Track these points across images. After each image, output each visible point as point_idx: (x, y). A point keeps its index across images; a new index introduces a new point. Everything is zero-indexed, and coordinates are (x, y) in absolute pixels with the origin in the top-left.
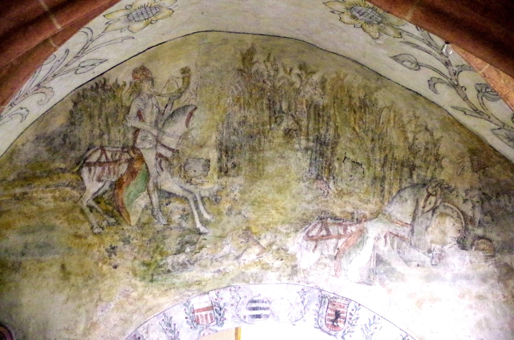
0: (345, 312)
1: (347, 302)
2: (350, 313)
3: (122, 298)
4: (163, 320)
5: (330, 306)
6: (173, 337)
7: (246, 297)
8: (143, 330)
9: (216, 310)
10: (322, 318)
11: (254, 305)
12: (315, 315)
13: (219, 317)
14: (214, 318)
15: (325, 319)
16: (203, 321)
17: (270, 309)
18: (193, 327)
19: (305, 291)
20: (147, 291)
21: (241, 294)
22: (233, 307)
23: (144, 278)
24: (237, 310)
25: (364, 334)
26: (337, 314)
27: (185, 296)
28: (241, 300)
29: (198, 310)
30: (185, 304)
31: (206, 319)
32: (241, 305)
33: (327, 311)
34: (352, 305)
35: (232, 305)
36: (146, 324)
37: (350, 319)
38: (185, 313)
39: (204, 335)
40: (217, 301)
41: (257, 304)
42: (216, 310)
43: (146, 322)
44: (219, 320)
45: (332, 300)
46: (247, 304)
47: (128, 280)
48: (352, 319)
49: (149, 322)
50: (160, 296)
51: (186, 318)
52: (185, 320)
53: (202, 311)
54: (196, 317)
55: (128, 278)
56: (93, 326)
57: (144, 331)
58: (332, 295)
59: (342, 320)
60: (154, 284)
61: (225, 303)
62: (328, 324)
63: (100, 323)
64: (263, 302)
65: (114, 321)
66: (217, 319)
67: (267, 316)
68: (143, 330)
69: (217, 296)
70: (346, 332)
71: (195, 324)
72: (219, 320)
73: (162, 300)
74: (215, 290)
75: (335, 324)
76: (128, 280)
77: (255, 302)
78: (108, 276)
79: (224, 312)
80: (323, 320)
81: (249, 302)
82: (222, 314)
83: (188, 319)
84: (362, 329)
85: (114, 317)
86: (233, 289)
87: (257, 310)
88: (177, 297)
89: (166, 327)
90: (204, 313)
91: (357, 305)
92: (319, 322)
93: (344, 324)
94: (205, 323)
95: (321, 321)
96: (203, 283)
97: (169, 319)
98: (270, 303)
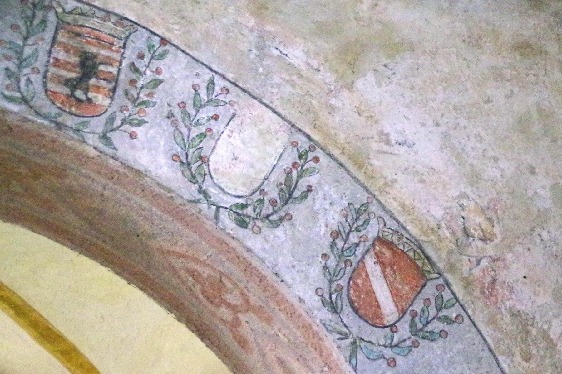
2: (133, 64)
5: (62, 38)
10: (36, 71)
12: (8, 58)
15: (45, 77)
25: (177, 133)
33: (50, 52)
37: (133, 82)
45: (69, 19)
48: (139, 85)
59: (103, 83)
62: (54, 93)
70: (118, 122)
75: (79, 93)
80: (36, 79)
84: (170, 116)
91: (156, 41)
92: (23, 84)
93: (112, 98)
95: (28, 80)
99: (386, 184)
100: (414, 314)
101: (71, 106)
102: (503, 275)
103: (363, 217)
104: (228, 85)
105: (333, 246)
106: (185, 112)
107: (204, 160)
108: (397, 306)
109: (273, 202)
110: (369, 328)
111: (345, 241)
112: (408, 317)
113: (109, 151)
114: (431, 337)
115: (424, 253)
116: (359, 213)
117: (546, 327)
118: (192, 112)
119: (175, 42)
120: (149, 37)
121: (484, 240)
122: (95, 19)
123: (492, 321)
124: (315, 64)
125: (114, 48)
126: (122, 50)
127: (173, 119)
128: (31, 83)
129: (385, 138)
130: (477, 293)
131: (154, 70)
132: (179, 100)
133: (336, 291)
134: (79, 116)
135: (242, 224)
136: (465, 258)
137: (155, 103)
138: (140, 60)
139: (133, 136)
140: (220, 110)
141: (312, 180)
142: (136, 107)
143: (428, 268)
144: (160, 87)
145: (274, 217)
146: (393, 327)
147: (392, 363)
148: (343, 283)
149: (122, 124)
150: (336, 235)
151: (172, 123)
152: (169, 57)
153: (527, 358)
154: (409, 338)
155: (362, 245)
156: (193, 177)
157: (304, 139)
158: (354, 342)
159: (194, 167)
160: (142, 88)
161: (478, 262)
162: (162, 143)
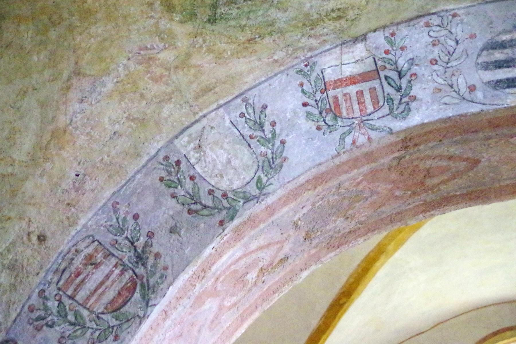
3: (132, 66)
4: (242, 115)
6: (270, 156)
7: (473, 36)
8: (189, 143)
9: (386, 77)
11: (499, 55)
14: (381, 98)
20: (201, 47)
22: (436, 67)
23: (193, 16)
24: (450, 71)
27: (303, 48)
28: (460, 48)
29: (339, 83)
30: (300, 71)
32: (459, 58)
35: (433, 62)
36: (198, 127)
38: (301, 94)
39: (354, 142)
40: (390, 56)
41: (508, 51)
42: (386, 77)
43: (197, 121)
44: (396, 102)
46: (479, 55)
47: (152, 21)
49: (204, 122)
50: (237, 54)
51: (305, 105)
52: (302, 111)
53: (347, 85)
54: (331, 100)
55: (151, 17)
57: (192, 145)
60: (219, 27)
61: (412, 59)
63: (76, 129)
65: (113, 123)
66: (390, 100)
68: (189, 143)
69: (391, 43)
71: (329, 119)
72: (396, 102)
74: (384, 27)
76: (152, 21)
78: (99, 15)
79: (410, 82)
81: (482, 50)
82: (404, 86)
83: (308, 108)
89: (251, 133)
90: (353, 89)
94: (357, 114)
96: (351, 14)
97: (258, 111)
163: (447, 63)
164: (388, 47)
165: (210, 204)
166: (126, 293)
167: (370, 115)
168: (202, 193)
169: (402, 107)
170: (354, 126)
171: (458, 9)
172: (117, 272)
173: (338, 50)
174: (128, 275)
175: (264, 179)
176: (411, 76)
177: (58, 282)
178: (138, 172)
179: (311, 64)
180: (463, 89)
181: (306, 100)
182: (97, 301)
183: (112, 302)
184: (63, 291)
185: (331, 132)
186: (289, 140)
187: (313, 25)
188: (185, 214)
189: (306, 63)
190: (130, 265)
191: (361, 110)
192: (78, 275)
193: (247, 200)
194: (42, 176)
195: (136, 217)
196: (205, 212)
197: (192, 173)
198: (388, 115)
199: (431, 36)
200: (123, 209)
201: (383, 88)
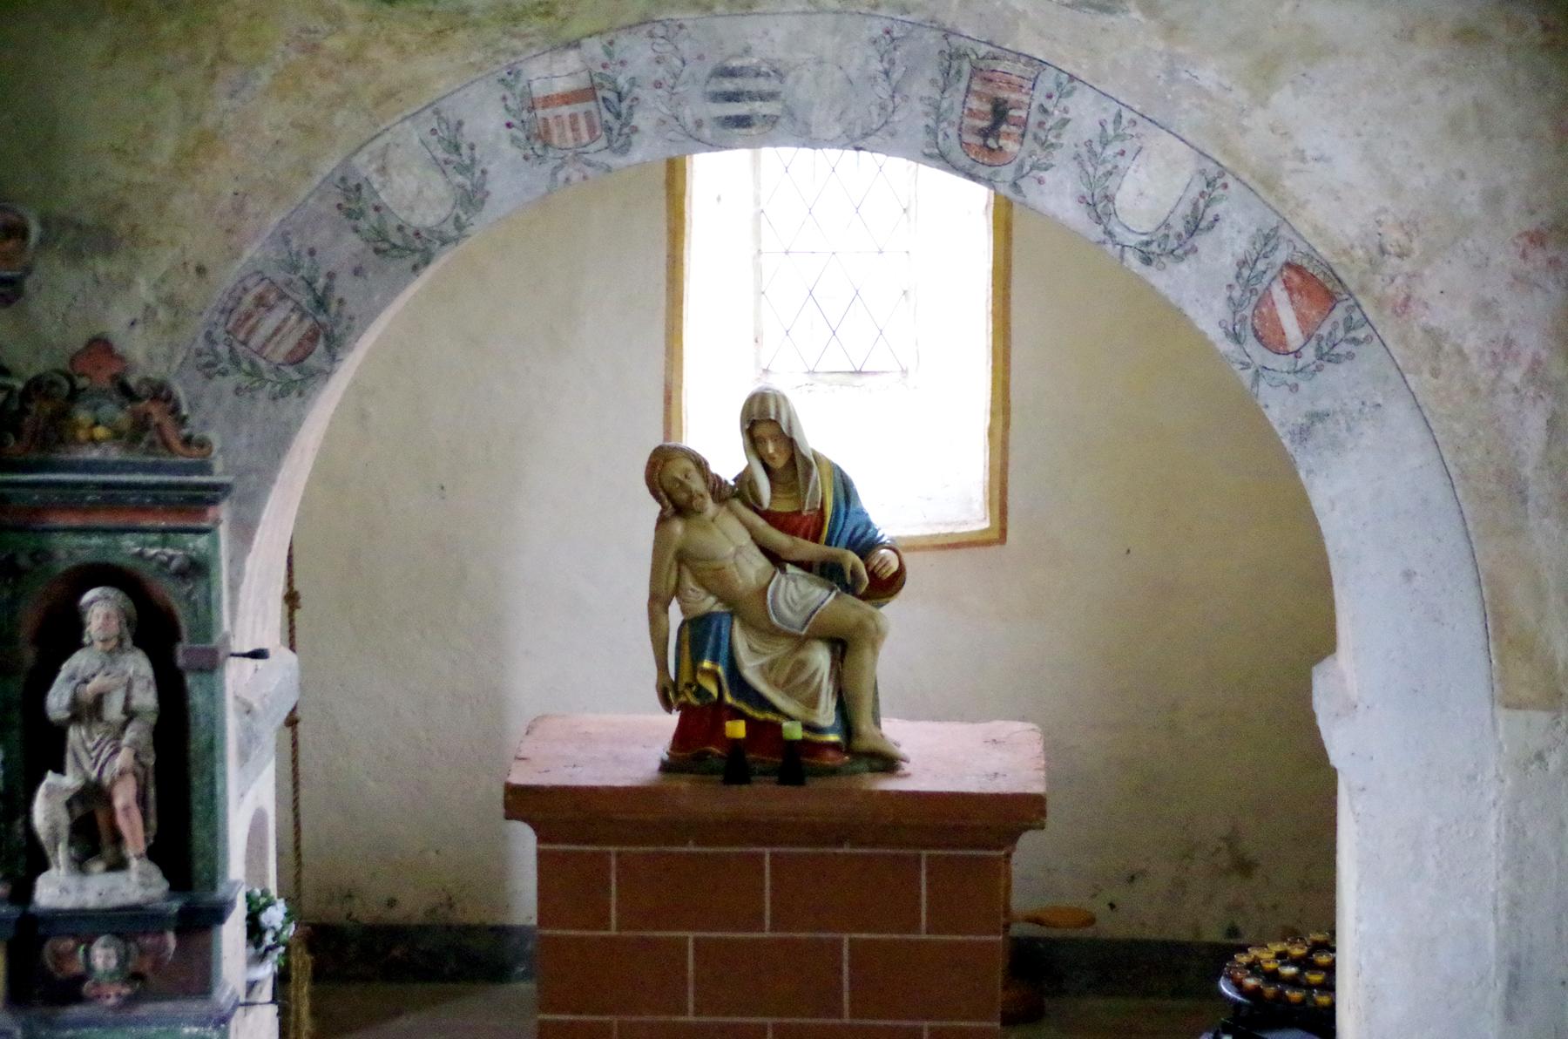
0: (1025, 105)
1: (1030, 72)
2: (1042, 105)
3: (293, 56)
4: (434, 131)
7: (700, 57)
8: (370, 161)
9: (604, 99)
10: (951, 124)
11: (729, 85)
12: (927, 114)
13: (616, 125)
15: (960, 129)
16: (562, 135)
17: (782, 96)
18: (533, 158)
19: (895, 34)
21: (685, 46)
22: (659, 92)
26: (1000, 112)
27: (503, 51)
28: (687, 70)
29: (548, 101)
30: (502, 80)
31: (574, 129)
32: (685, 83)
33: (964, 102)
34: (1047, 82)
35: (658, 85)
36: (380, 142)
37: (1041, 124)
38: (503, 111)
39: (567, 180)
40: (608, 72)
43: (376, 136)
45: (982, 65)
48: (1047, 126)
49: (388, 137)
51: (509, 125)
53: (559, 105)
54: (541, 123)
56: (207, 142)
57: (374, 166)
58: (983, 50)
59: (1013, 129)
64: (758, 75)
66: (610, 129)
67: (772, 121)
69: (609, 54)
70: (1027, 168)
71: (538, 146)
72: (615, 132)
73: (428, 65)
75: (991, 142)
77: (731, 73)
79: (631, 107)
80: (952, 132)
82: (624, 112)
83: (513, 130)
84: (1077, 157)
85: (273, 117)
86: (659, 31)
87: (738, 101)
88: (476, 57)
89: (446, 156)
90: (565, 111)
91: (1064, 78)
93: (1022, 144)
94: (571, 144)
95: (946, 135)
97: (452, 127)
98: (779, 75)
99: (1298, 205)
100: (1320, 338)
101: (983, 157)
102: (1420, 292)
103: (1272, 243)
104: (1135, 116)
105: (1238, 277)
106: (1091, 151)
107: (1109, 198)
108: (1303, 332)
109: (1179, 236)
110: (1270, 355)
111: (1252, 269)
112: (1314, 341)
113: (1019, 198)
114: (1337, 359)
115: (1335, 275)
116: (1267, 238)
117: (1459, 341)
118: (1098, 149)
119: (1083, 78)
120: (1058, 75)
121: (1400, 256)
122: (1006, 62)
123: (1403, 340)
124: (1227, 82)
125: (1023, 91)
126: (1031, 92)
127: (1080, 159)
128: (948, 136)
129: (1301, 156)
130: (1388, 312)
131: (1062, 109)
132: (1086, 138)
133: (1240, 321)
134: (990, 166)
135: (1147, 260)
136: (1378, 278)
137: (1062, 145)
138: (1047, 100)
139: (1040, 181)
140: (1128, 145)
141: (1218, 208)
142: (1045, 150)
143: (1339, 289)
144: (1068, 127)
145: (1179, 252)
146: (1297, 354)
147: (1294, 388)
148: (1248, 312)
149: (1031, 169)
150: (1242, 264)
151: (1079, 163)
152: (1077, 94)
153: (1435, 373)
154: (1314, 363)
155: (1269, 272)
156: (1099, 217)
157: (1213, 165)
158: (1257, 371)
159: (1100, 207)
160: (1050, 130)
161: (1393, 281)
162: (1068, 186)
163: (673, 88)
164: (605, 59)
165: (399, 242)
166: (306, 342)
167: (585, 146)
168: (391, 233)
169: (622, 140)
170: (567, 158)
171: (685, 19)
172: (294, 317)
173: (546, 57)
174: (308, 323)
175: (464, 217)
176: (632, 101)
177: (226, 324)
178: (311, 195)
179: (515, 72)
180: (690, 125)
181: (511, 119)
182: (273, 351)
183: (292, 352)
184: (233, 335)
185: (540, 164)
186: (491, 169)
187: (516, 19)
188: (371, 255)
189: (509, 70)
190: (310, 311)
191: (576, 140)
192: (249, 316)
193: (444, 243)
194: (192, 191)
195: (312, 252)
196: (395, 252)
197: (375, 202)
198: (606, 148)
199: (654, 50)
200: (295, 244)
201: (600, 113)
